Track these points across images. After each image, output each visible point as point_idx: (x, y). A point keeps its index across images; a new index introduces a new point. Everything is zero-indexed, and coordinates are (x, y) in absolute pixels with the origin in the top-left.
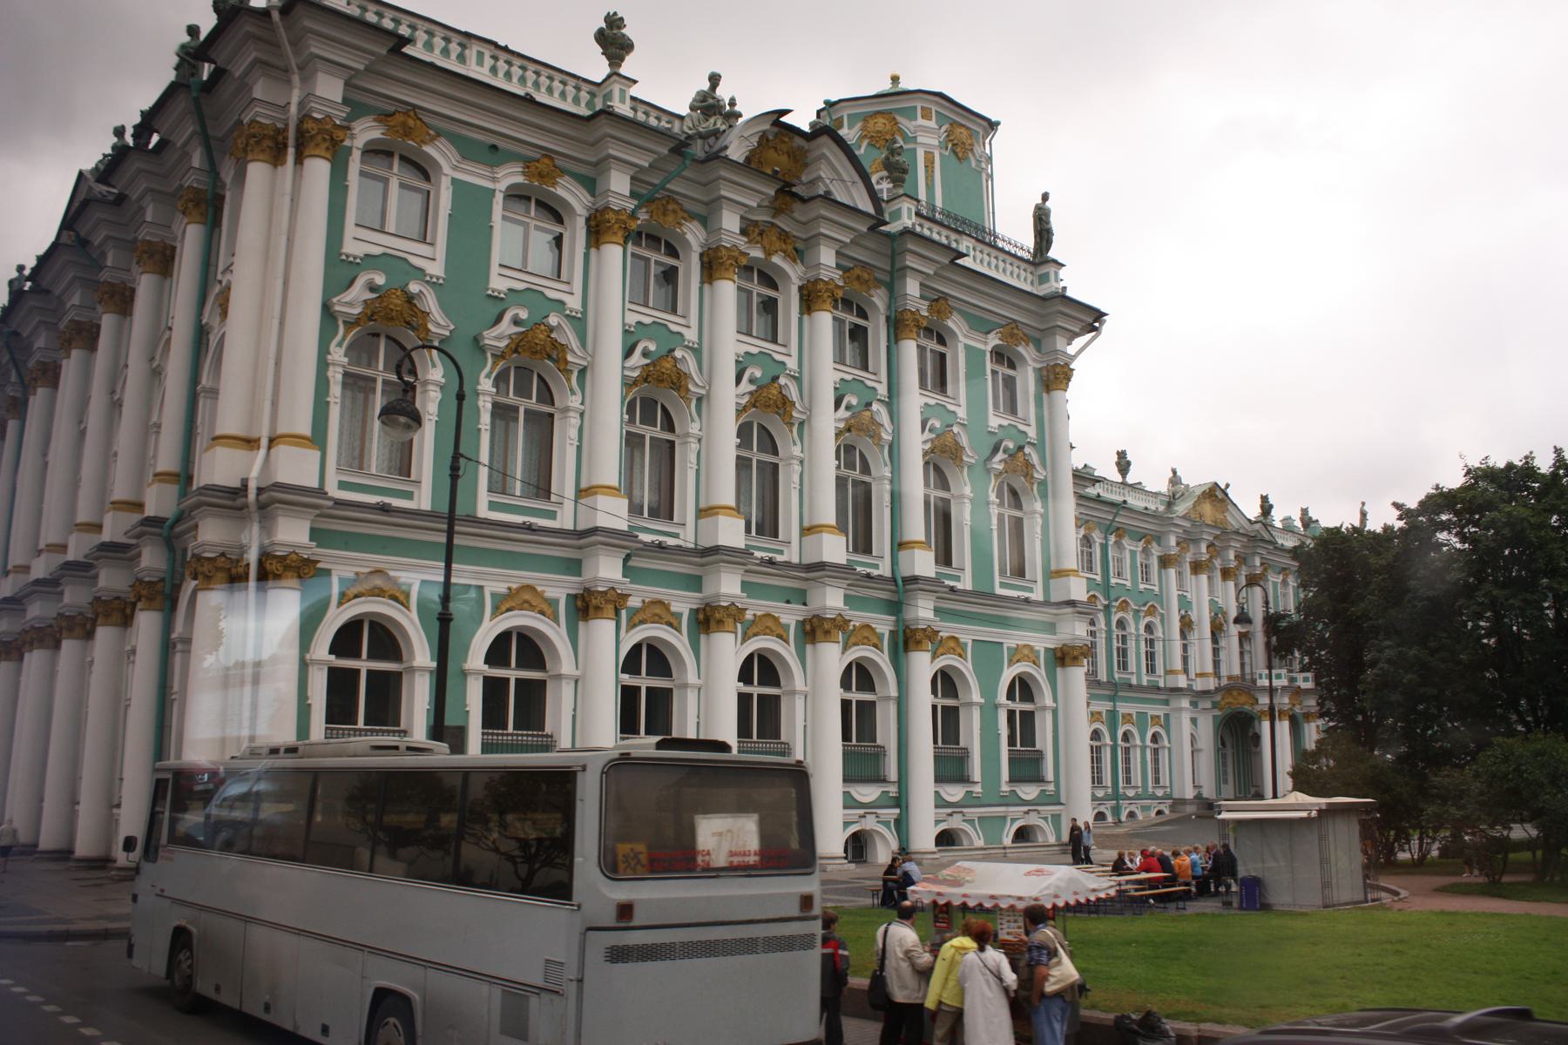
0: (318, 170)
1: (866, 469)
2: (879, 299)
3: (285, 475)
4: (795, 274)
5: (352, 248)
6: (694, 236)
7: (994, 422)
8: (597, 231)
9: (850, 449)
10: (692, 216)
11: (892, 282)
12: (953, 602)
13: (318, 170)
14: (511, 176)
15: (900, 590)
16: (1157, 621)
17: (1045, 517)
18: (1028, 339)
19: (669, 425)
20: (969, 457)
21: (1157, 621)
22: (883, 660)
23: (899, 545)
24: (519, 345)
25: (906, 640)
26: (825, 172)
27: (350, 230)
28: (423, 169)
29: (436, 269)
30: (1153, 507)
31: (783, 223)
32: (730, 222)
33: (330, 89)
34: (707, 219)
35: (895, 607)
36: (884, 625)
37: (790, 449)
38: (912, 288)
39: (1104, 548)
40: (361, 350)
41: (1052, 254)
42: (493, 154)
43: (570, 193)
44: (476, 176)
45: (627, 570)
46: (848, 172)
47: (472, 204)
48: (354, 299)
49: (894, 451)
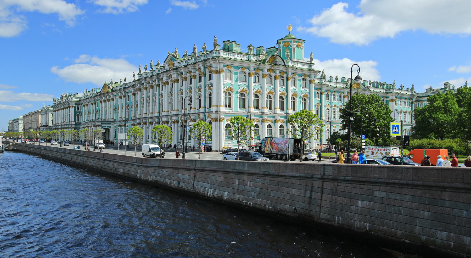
17: (310, 102)
18: (308, 76)
26: (278, 61)
27: (224, 81)
31: (272, 68)
33: (222, 65)
41: (312, 62)
43: (247, 71)
44: (236, 71)
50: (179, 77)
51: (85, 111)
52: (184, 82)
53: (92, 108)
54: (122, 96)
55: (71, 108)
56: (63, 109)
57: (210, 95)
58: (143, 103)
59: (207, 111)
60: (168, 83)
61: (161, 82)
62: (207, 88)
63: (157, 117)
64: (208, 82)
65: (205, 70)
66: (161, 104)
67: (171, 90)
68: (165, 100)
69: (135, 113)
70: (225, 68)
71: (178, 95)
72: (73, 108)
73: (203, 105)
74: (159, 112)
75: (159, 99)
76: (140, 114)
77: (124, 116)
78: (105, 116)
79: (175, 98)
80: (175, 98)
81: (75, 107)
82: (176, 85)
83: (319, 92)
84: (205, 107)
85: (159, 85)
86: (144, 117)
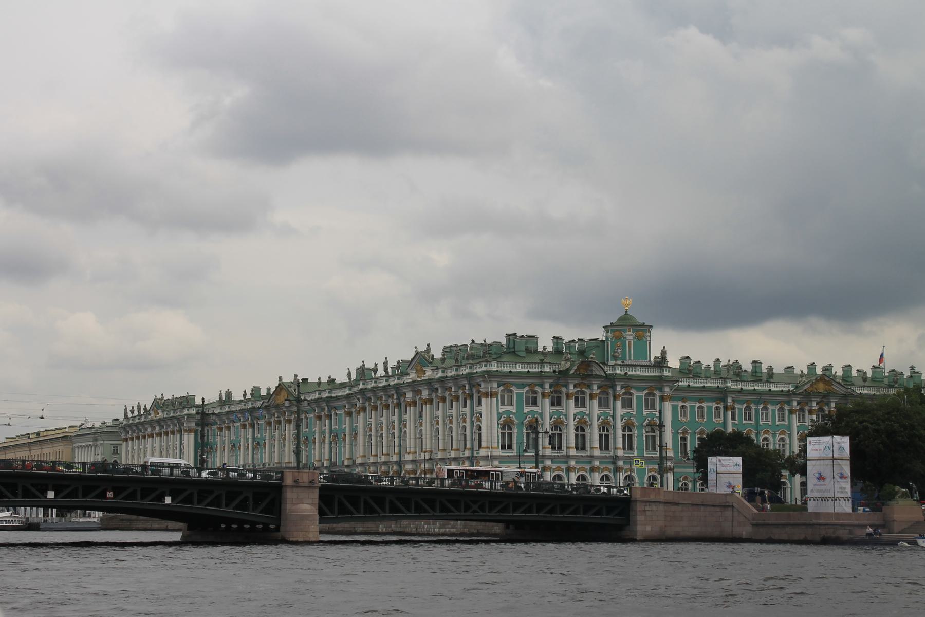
0: (495, 400)
1: (608, 431)
2: (610, 391)
3: (495, 454)
4: (588, 391)
5: (500, 411)
6: (564, 390)
7: (645, 413)
8: (544, 395)
9: (603, 428)
10: (563, 386)
11: (613, 387)
12: (629, 461)
13: (495, 400)
14: (527, 389)
15: (614, 460)
16: (787, 438)
19: (560, 430)
20: (636, 424)
21: (787, 438)
22: (611, 475)
23: (615, 448)
24: (530, 422)
25: (617, 470)
28: (511, 391)
29: (514, 411)
30: (785, 389)
32: (571, 387)
33: (495, 385)
34: (566, 386)
35: (614, 463)
36: (611, 467)
37: (588, 431)
38: (618, 388)
39: (757, 410)
40: (503, 428)
42: (522, 386)
43: (538, 389)
44: (520, 391)
45: (552, 462)
46: (599, 368)
47: (519, 395)
48: (501, 422)
49: (614, 426)
50: (434, 395)
51: (223, 443)
52: (441, 404)
53: (245, 436)
54: (323, 414)
55: (186, 436)
56: (160, 435)
57: (480, 429)
58: (370, 435)
59: (475, 454)
60: (414, 403)
61: (402, 399)
62: (475, 419)
63: (396, 462)
64: (477, 409)
65: (471, 389)
66: (403, 436)
67: (421, 416)
68: (410, 429)
69: (351, 452)
70: (501, 388)
71: (432, 425)
72: (192, 435)
73: (468, 446)
74: (400, 453)
75: (400, 429)
76: (365, 456)
77: (327, 458)
78: (280, 457)
79: (426, 428)
80: (426, 428)
81: (196, 432)
82: (427, 409)
83: (721, 406)
84: (472, 449)
85: (399, 405)
86: (371, 461)
